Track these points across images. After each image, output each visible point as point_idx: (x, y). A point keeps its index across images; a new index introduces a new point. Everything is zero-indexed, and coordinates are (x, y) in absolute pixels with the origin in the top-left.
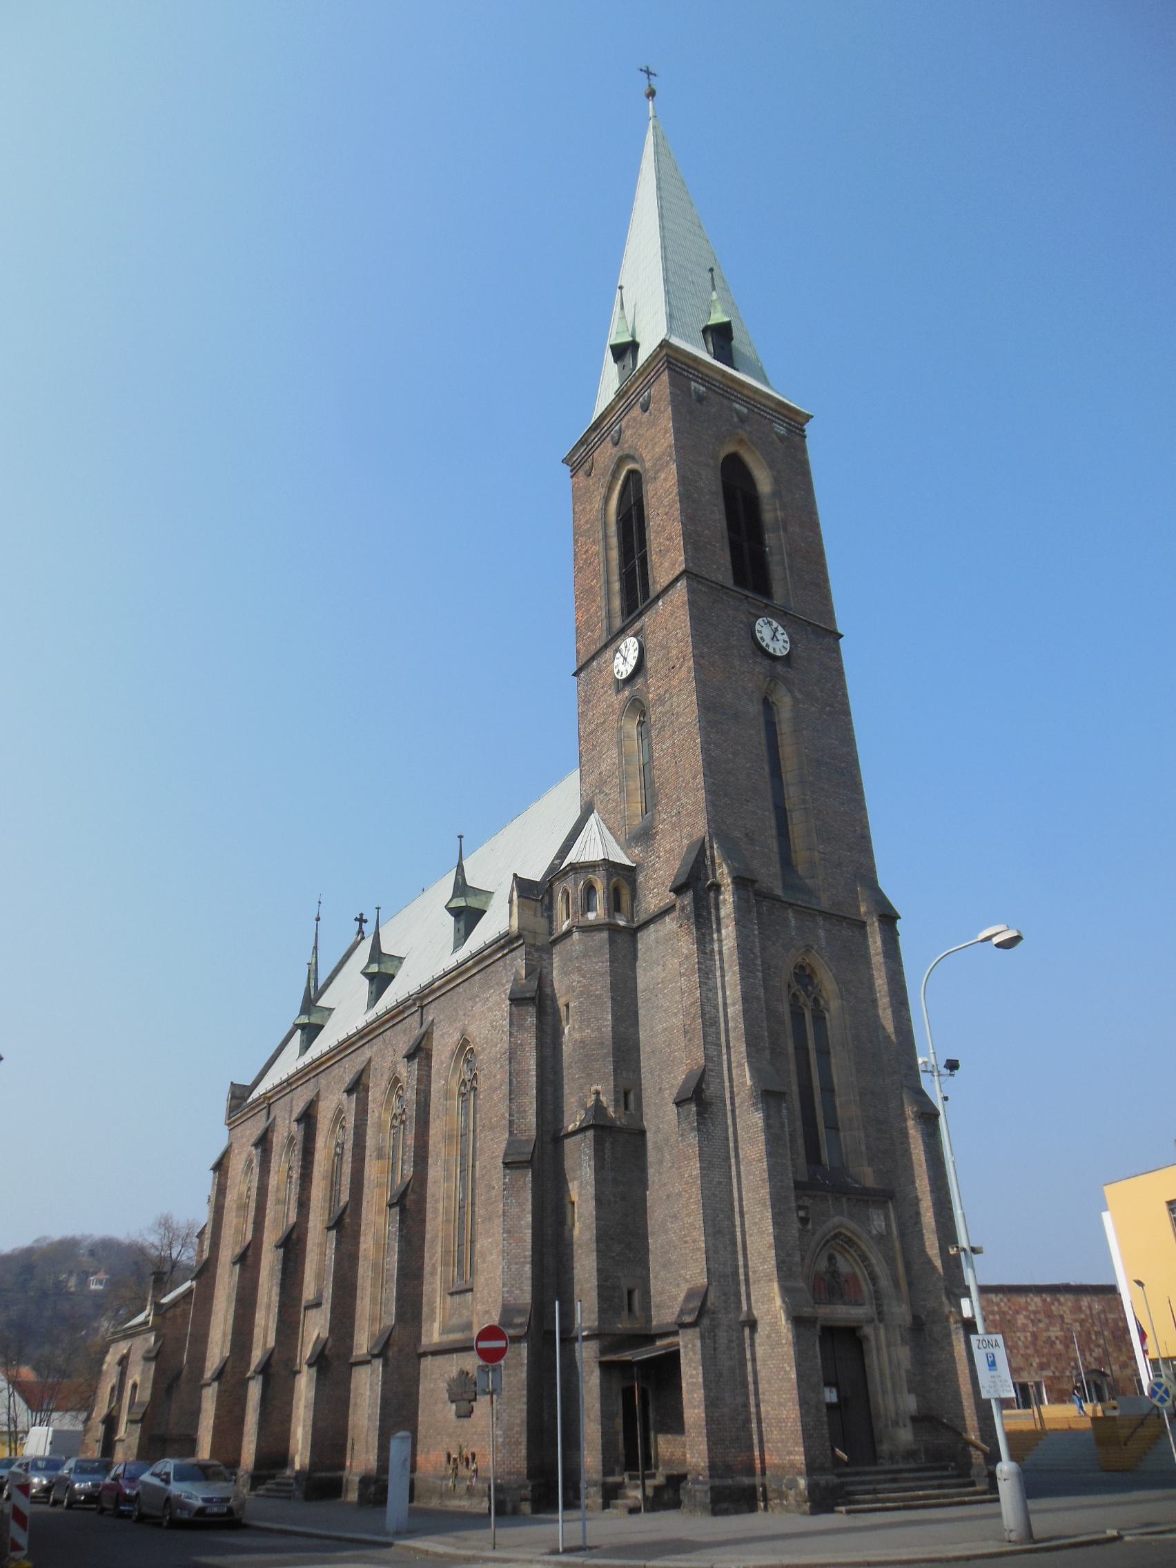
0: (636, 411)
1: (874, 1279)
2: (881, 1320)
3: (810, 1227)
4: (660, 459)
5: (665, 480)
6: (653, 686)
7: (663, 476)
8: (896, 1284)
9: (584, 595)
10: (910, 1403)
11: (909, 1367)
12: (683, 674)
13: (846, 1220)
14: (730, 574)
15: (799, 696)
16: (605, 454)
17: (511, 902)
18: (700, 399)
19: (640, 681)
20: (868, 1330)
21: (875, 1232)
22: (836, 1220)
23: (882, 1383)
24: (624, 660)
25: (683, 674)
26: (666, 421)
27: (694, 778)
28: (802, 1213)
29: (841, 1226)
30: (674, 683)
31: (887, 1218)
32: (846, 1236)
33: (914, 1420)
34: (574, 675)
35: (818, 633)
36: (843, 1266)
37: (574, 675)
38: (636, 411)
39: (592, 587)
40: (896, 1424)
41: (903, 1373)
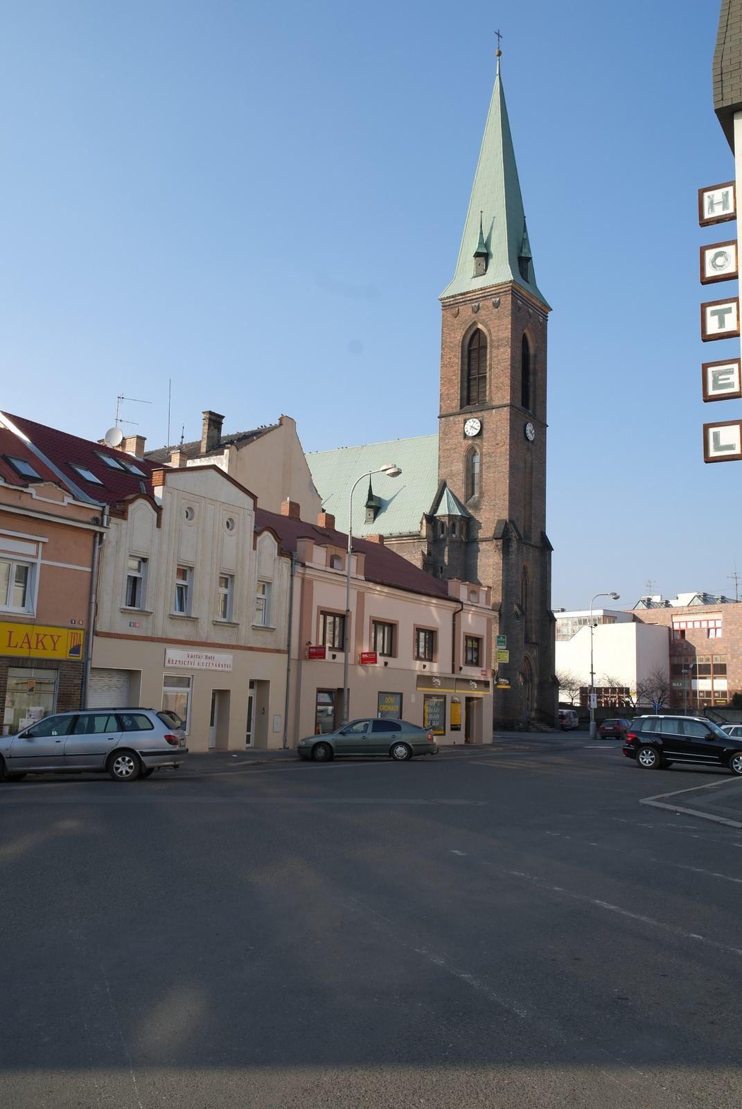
0: (489, 303)
1: (531, 670)
4: (502, 340)
5: (504, 353)
6: (486, 446)
7: (502, 350)
9: (445, 380)
12: (503, 449)
14: (521, 403)
15: (534, 457)
16: (466, 312)
17: (421, 523)
18: (520, 309)
19: (478, 441)
24: (472, 427)
25: (503, 449)
26: (507, 321)
27: (504, 495)
30: (498, 451)
34: (439, 417)
35: (541, 426)
37: (439, 417)
38: (489, 303)
39: (452, 379)
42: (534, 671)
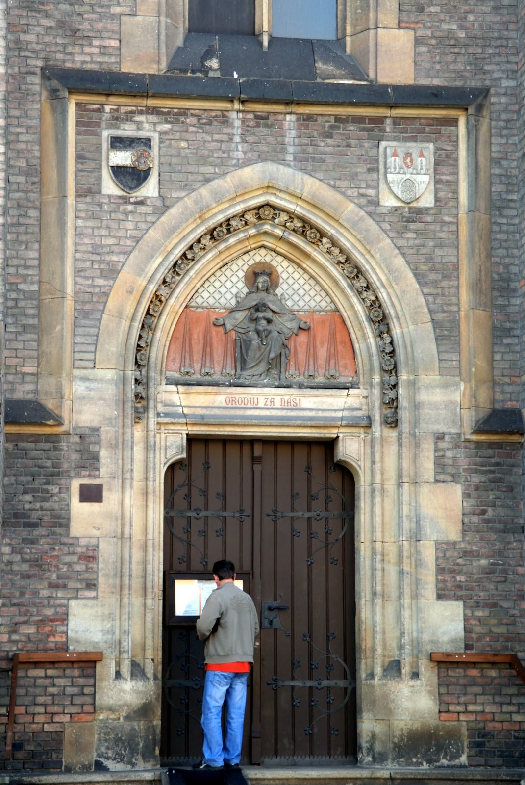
1: (381, 321)
2: (393, 422)
3: (150, 189)
8: (446, 332)
10: (445, 623)
11: (454, 534)
13: (284, 173)
20: (350, 448)
21: (388, 202)
22: (251, 174)
23: (373, 576)
28: (123, 158)
29: (269, 188)
31: (444, 162)
32: (292, 216)
33: (444, 663)
36: (300, 290)
40: (394, 668)
41: (429, 554)
42: (413, 329)
